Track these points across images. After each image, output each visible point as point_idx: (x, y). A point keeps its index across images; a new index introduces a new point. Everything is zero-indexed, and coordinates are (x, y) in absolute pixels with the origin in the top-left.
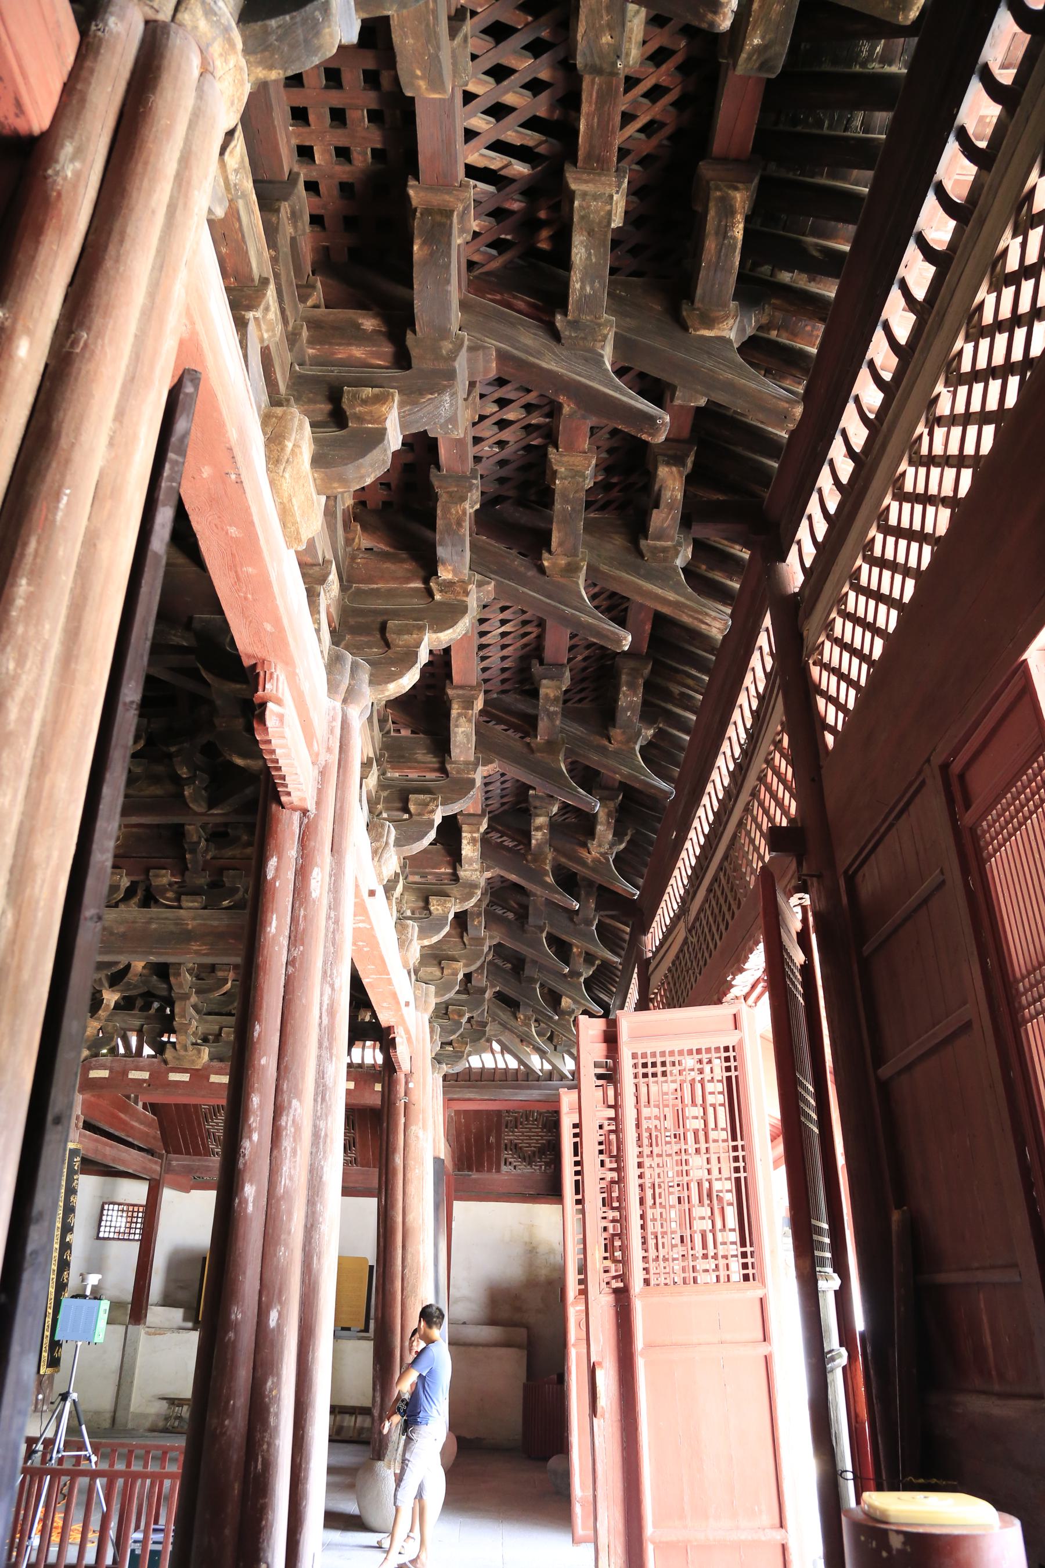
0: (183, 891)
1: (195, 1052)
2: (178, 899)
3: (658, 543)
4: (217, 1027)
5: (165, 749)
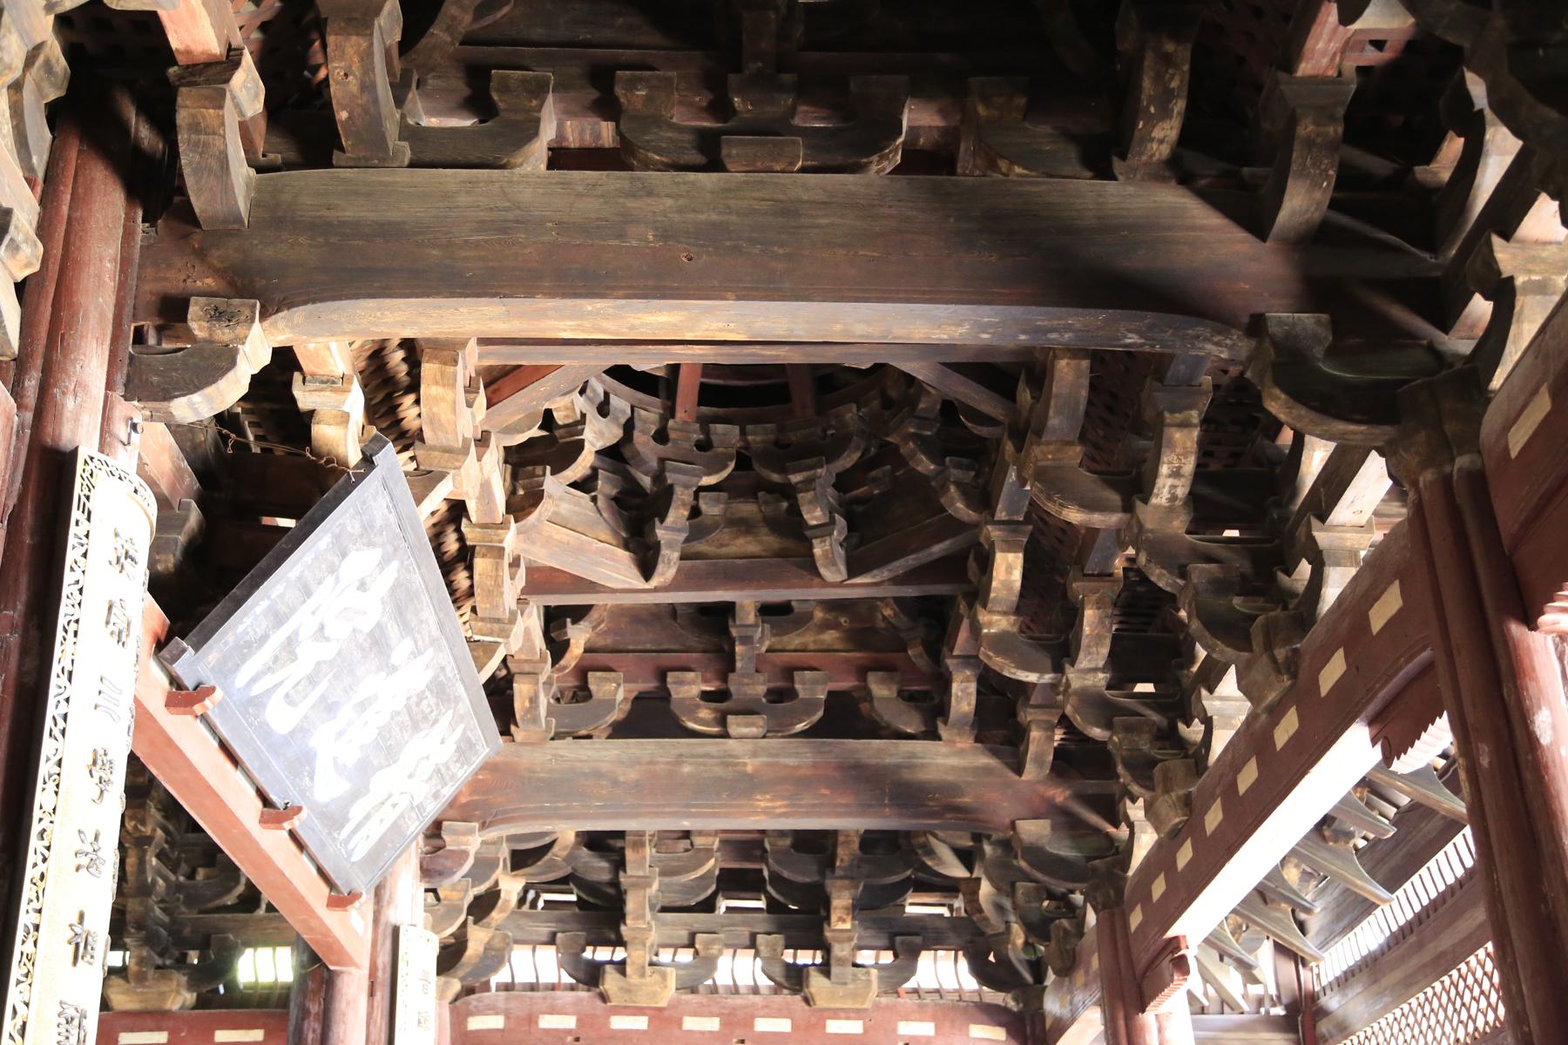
1: (656, 977)
2: (723, 722)
4: (683, 935)
5: (776, 477)
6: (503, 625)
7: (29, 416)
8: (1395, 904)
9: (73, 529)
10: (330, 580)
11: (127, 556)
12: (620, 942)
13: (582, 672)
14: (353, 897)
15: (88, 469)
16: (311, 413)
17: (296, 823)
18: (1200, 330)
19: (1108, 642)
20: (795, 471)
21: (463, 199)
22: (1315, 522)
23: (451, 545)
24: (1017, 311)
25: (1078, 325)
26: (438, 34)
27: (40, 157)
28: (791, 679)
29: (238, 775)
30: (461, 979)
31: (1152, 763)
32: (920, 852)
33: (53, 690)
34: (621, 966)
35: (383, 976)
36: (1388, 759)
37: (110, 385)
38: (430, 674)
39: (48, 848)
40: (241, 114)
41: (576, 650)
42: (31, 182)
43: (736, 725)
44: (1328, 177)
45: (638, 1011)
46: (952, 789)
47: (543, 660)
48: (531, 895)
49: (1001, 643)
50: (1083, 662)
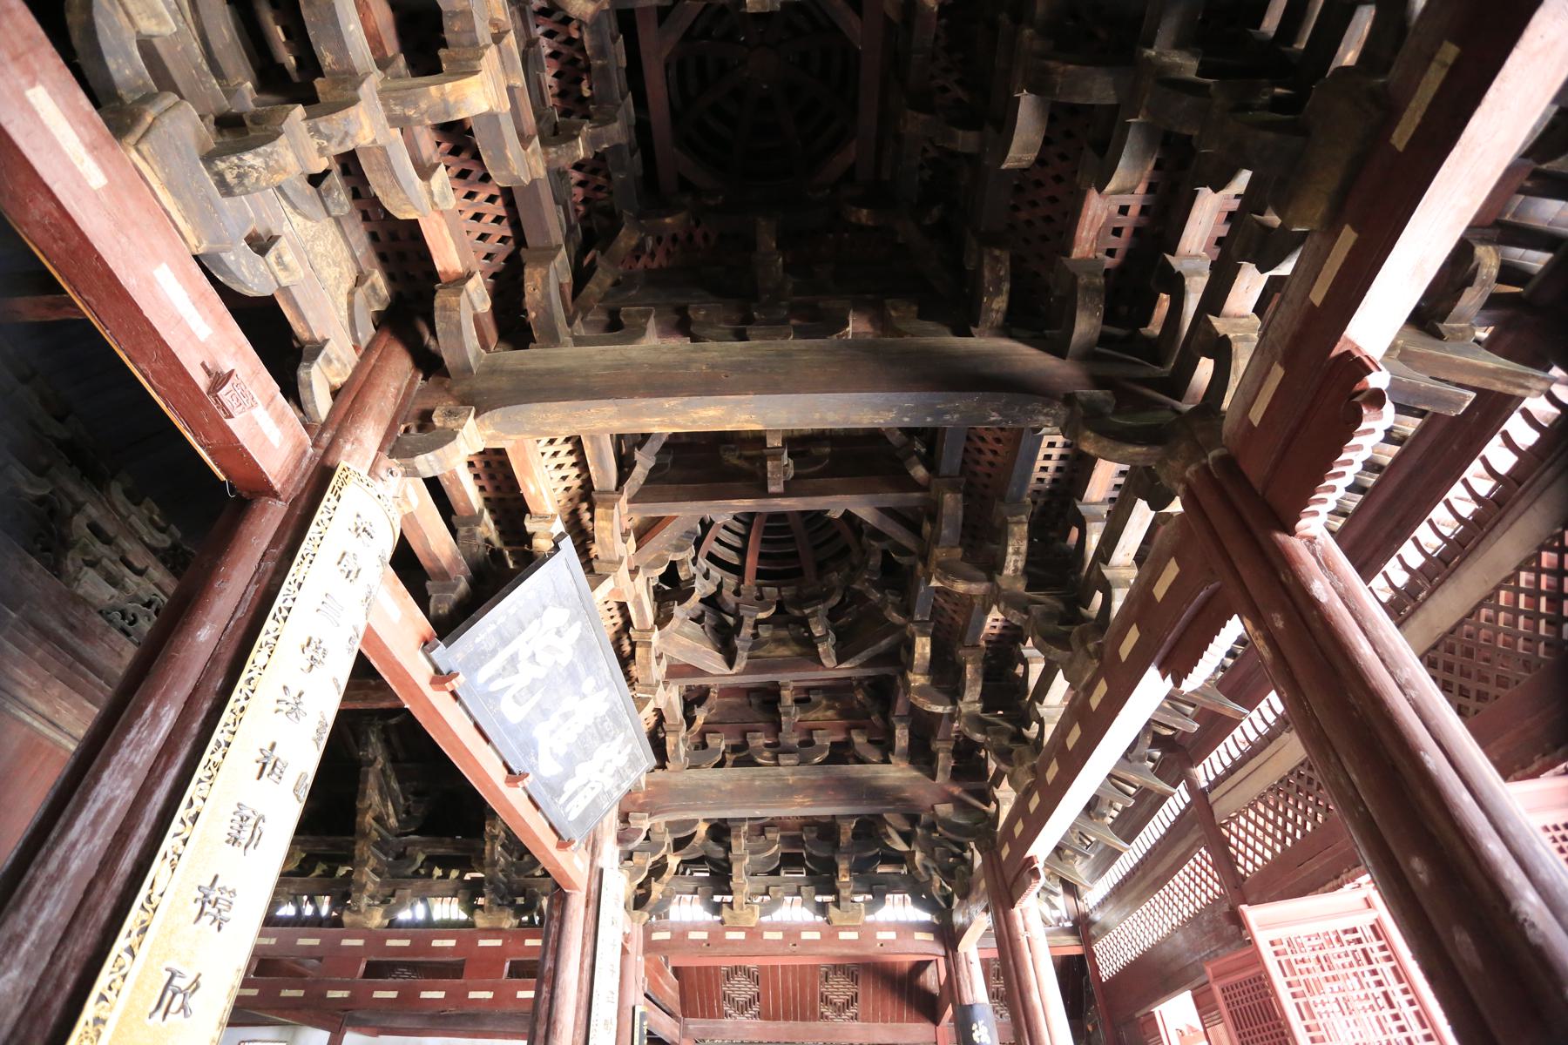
0: (777, 749)
2: (776, 758)
3: (1455, 325)
4: (762, 888)
5: (797, 613)
6: (651, 688)
7: (321, 452)
8: (1131, 851)
9: (324, 502)
10: (536, 622)
11: (364, 530)
12: (730, 893)
13: (703, 734)
14: (571, 842)
15: (345, 474)
16: (534, 534)
17: (526, 782)
18: (1037, 406)
19: (980, 683)
20: (807, 607)
21: (598, 357)
22: (1102, 565)
23: (627, 648)
24: (924, 396)
25: (962, 408)
26: (592, 287)
27: (365, 336)
28: (811, 735)
29: (489, 748)
30: (650, 913)
31: (1011, 751)
33: (283, 591)
34: (730, 905)
35: (593, 896)
36: (1177, 683)
37: (380, 449)
38: (607, 706)
39: (253, 691)
40: (474, 308)
41: (700, 721)
42: (356, 348)
43: (783, 759)
44: (1099, 309)
45: (740, 929)
46: (899, 789)
47: (681, 724)
48: (688, 872)
49: (921, 691)
50: (968, 697)
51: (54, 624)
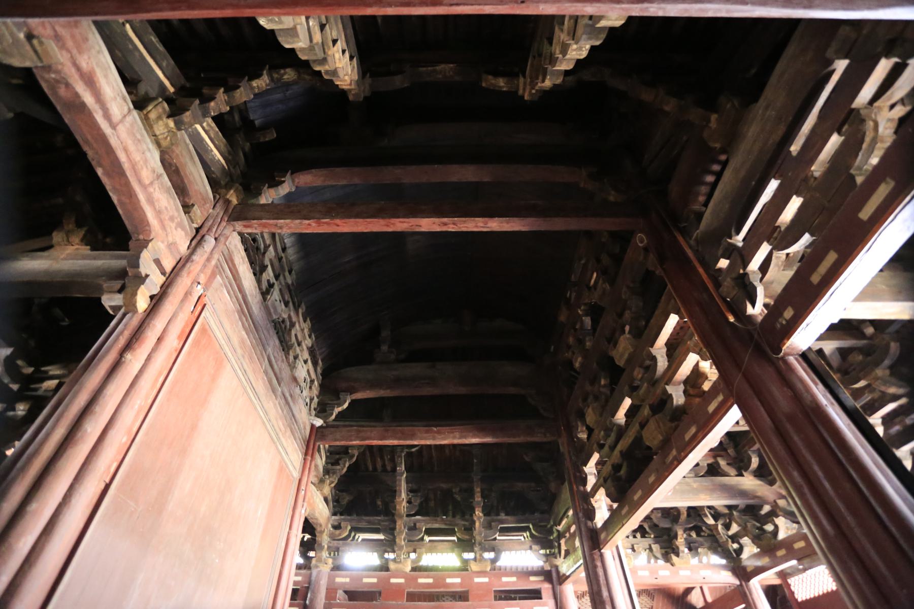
32: (703, 516)
51: (287, 395)
